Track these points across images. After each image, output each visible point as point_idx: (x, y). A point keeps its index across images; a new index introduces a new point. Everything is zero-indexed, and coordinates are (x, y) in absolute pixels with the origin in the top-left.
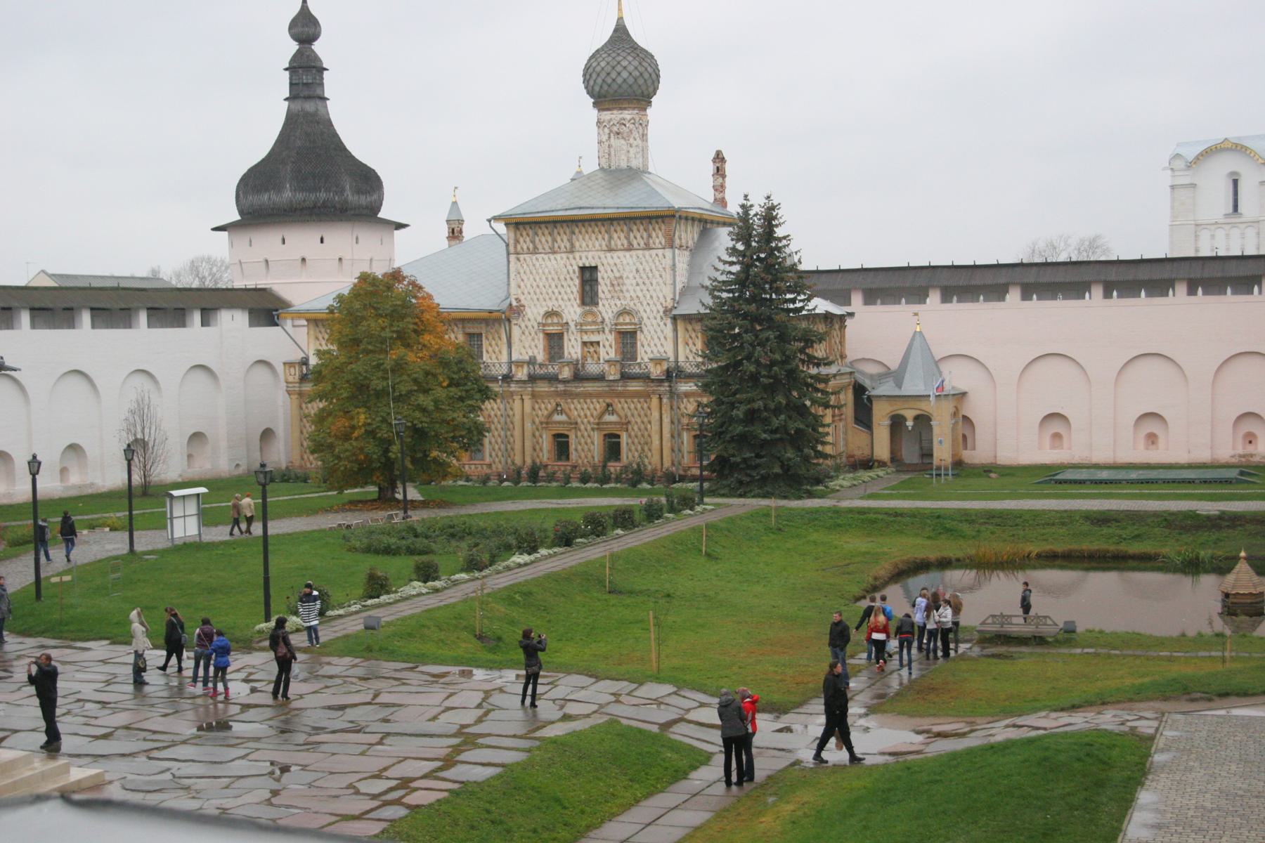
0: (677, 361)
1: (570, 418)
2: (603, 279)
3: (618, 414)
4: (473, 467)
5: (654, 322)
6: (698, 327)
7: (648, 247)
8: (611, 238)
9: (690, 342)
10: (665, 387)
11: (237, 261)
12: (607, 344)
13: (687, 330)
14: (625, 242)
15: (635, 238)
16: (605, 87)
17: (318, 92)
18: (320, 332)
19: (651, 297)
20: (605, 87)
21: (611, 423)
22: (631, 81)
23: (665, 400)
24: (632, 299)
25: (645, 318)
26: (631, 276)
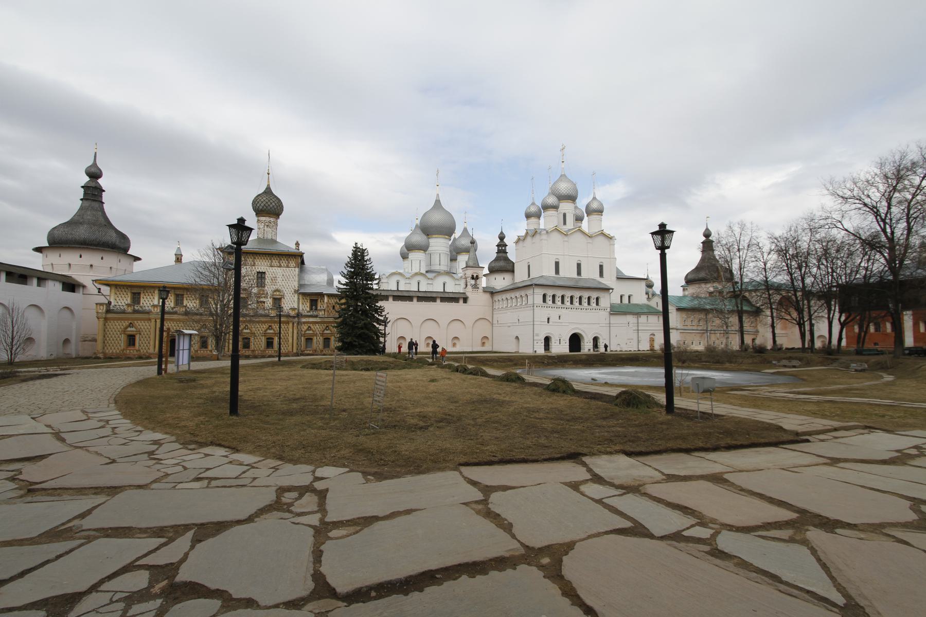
0: (299, 310)
1: (251, 331)
2: (268, 277)
3: (274, 330)
4: (202, 351)
5: (289, 295)
6: (308, 298)
7: (288, 267)
8: (272, 262)
9: (304, 303)
10: (296, 319)
11: (50, 263)
12: (268, 302)
13: (303, 299)
14: (278, 264)
15: (283, 262)
16: (265, 208)
17: (100, 199)
18: (118, 291)
19: (289, 285)
20: (265, 208)
21: (270, 333)
22: (276, 207)
23: (295, 325)
24: (280, 286)
25: (286, 294)
26: (280, 277)
